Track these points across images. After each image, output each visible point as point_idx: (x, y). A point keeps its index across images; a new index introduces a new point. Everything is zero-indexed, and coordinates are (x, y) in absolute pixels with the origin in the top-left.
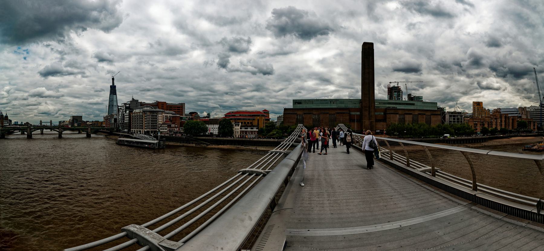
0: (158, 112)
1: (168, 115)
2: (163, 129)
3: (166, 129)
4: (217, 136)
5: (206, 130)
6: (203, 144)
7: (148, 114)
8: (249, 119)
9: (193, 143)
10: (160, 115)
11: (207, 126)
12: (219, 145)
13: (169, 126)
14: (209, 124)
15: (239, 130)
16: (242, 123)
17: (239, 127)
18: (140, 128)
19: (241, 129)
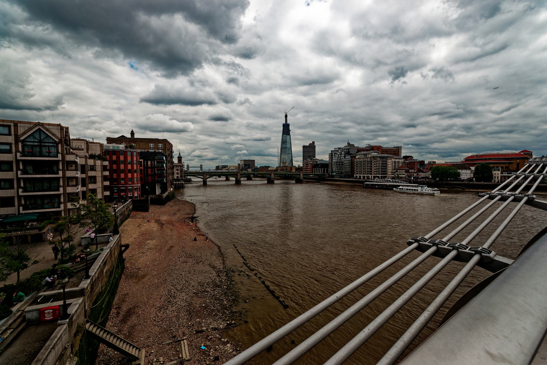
0: (388, 157)
2: (401, 174)
3: (403, 174)
4: (470, 180)
5: (459, 174)
6: (458, 188)
7: (378, 159)
8: (504, 163)
9: (444, 187)
10: (389, 161)
11: (460, 171)
12: (478, 189)
13: (407, 171)
14: (462, 169)
15: (500, 175)
16: (501, 167)
17: (499, 172)
18: (368, 174)
19: (501, 173)
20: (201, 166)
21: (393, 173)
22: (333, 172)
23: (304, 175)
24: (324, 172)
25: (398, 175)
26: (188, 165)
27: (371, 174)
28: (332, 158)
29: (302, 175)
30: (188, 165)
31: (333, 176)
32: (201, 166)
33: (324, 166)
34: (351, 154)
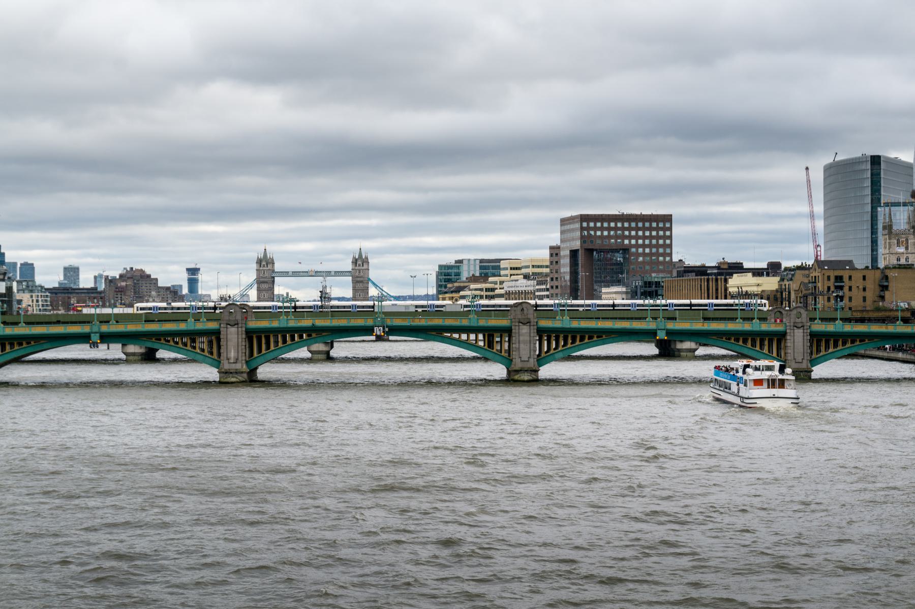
20: (360, 261)
26: (265, 263)
30: (265, 263)
32: (360, 261)
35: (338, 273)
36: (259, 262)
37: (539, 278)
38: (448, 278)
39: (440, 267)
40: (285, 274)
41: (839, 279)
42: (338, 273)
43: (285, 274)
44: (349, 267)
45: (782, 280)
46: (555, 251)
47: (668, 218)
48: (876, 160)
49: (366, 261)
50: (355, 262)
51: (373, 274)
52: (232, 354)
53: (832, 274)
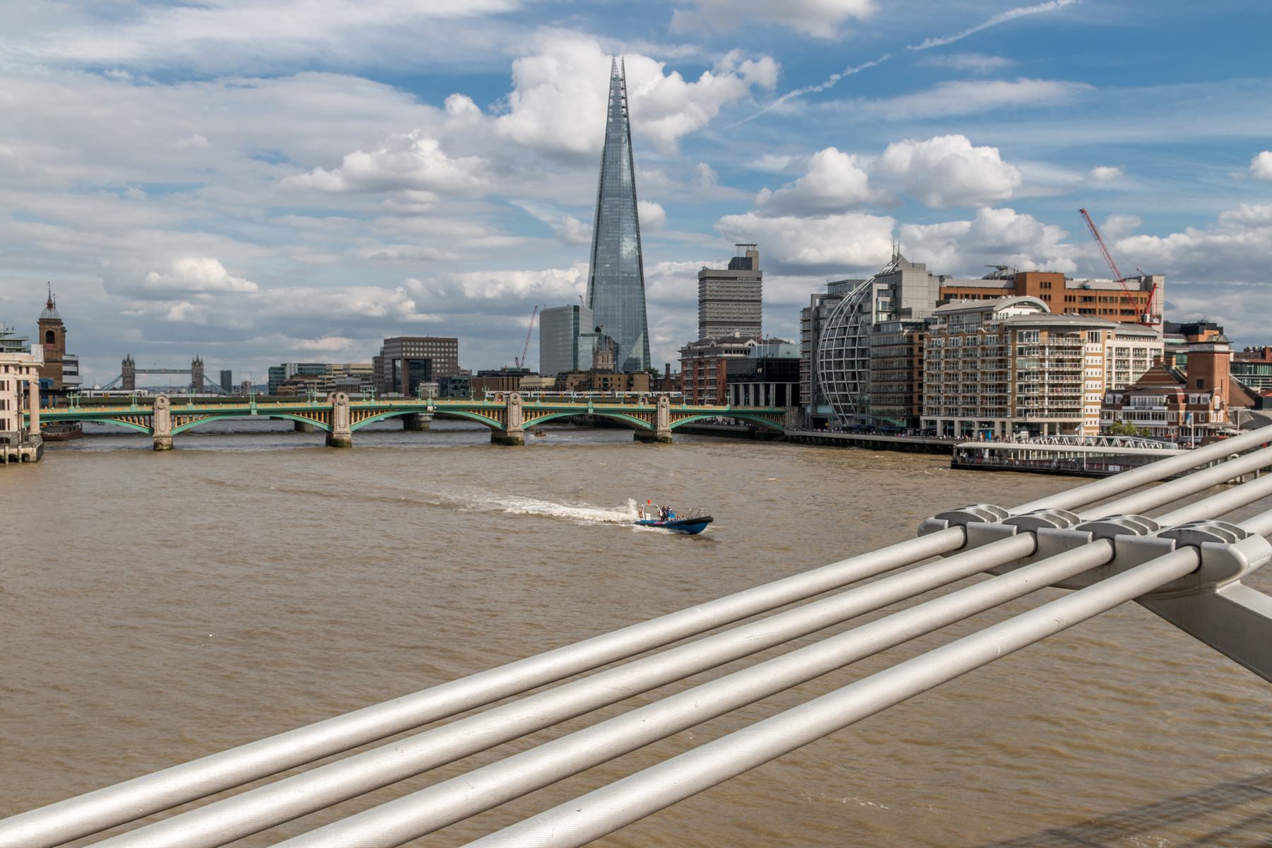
1: (1131, 344)
2: (1144, 417)
3: (1161, 417)
10: (1089, 346)
20: (198, 364)
21: (1108, 407)
22: (820, 401)
23: (674, 414)
24: (780, 401)
25: (1129, 416)
26: (128, 364)
27: (1001, 412)
28: (817, 330)
29: (664, 415)
30: (128, 364)
31: (820, 422)
32: (198, 364)
33: (780, 373)
34: (908, 312)
35: (182, 372)
36: (124, 363)
37: (365, 377)
38: (277, 373)
39: (271, 370)
40: (144, 371)
41: (605, 379)
42: (182, 372)
43: (144, 371)
44: (190, 367)
45: (558, 380)
46: (378, 361)
47: (455, 341)
48: (576, 309)
49: (201, 364)
50: (194, 364)
51: (205, 374)
52: (342, 423)
53: (602, 376)
